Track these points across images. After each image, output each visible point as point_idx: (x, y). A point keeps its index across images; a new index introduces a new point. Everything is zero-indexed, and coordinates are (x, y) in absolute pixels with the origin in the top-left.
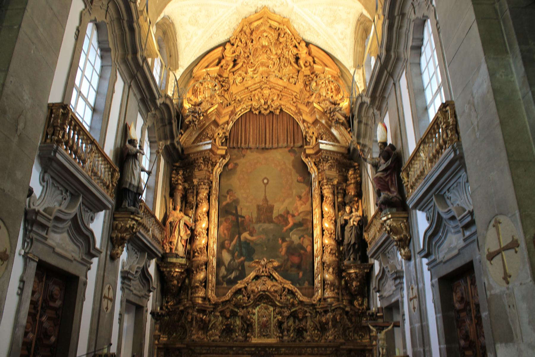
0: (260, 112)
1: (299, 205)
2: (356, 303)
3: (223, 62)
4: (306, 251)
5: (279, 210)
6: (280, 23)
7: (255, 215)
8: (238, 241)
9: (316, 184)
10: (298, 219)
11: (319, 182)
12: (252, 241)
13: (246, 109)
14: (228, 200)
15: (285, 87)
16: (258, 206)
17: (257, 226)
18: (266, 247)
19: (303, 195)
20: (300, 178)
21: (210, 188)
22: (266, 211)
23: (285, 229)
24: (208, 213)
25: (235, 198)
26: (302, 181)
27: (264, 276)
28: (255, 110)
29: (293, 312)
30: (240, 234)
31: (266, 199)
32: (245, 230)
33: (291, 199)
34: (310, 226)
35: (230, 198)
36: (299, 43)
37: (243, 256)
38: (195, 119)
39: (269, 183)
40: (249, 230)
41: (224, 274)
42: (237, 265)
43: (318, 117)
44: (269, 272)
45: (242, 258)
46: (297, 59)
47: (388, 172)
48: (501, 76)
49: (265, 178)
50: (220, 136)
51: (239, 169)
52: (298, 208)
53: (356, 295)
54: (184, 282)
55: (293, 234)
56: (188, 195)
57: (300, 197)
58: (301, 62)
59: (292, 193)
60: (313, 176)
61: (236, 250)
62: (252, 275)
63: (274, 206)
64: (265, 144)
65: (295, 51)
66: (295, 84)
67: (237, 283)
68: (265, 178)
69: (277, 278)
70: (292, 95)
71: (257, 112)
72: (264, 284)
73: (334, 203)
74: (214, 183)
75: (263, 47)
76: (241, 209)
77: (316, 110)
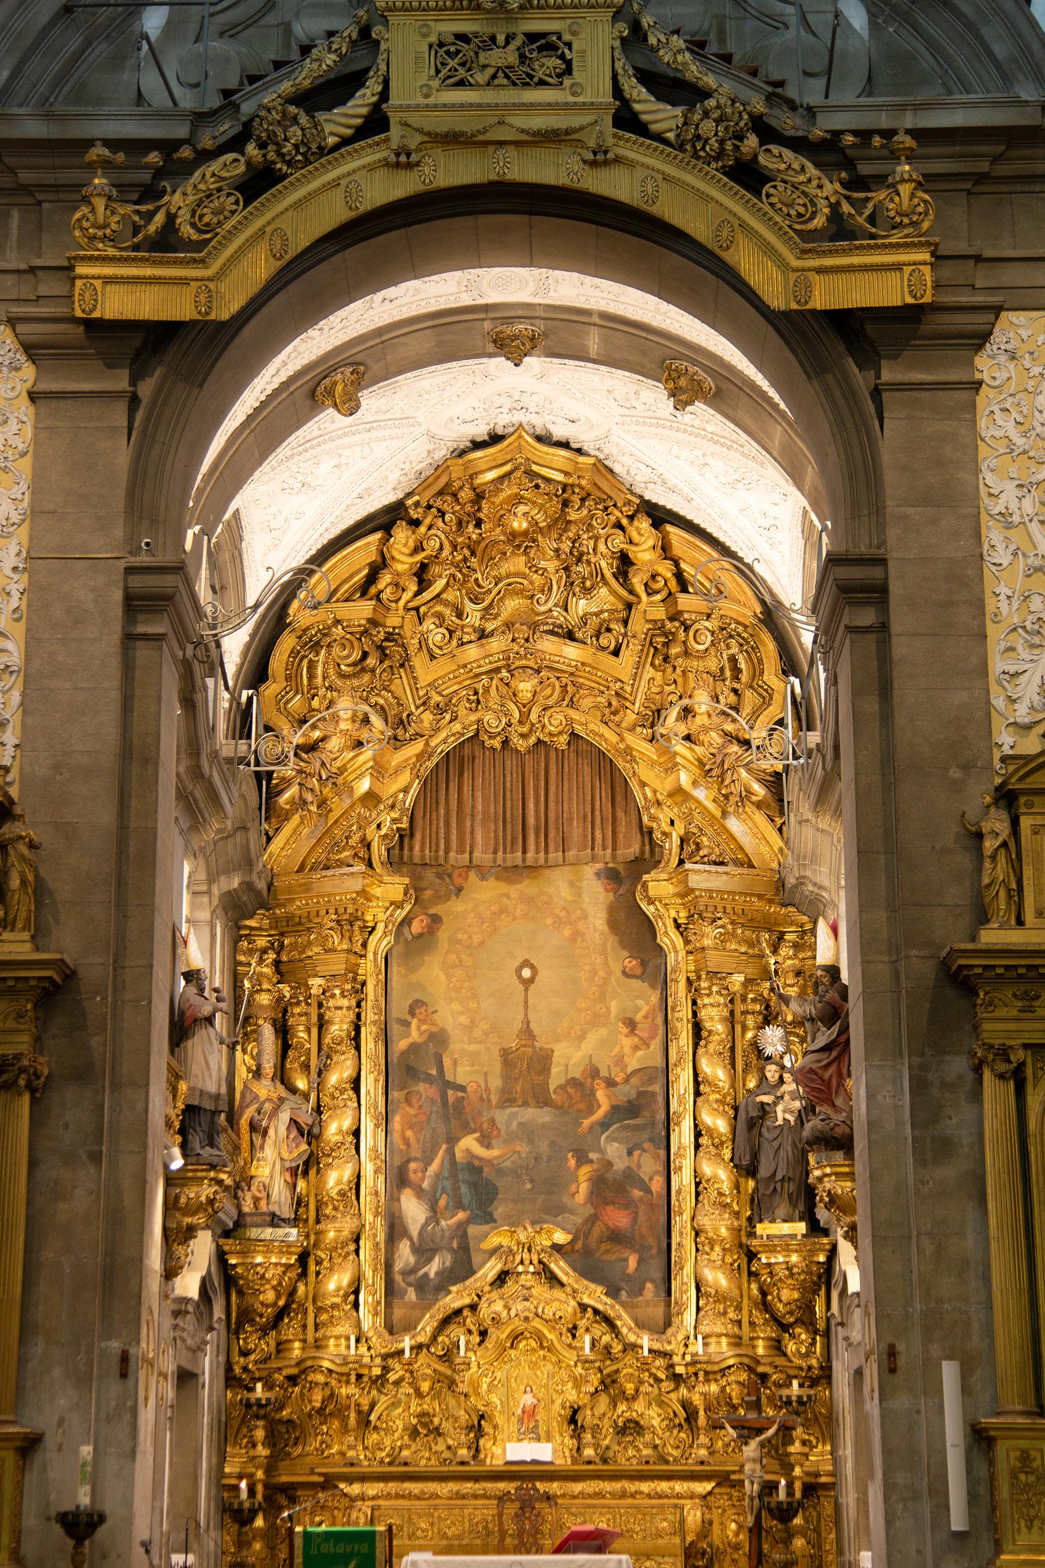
0: (505, 743)
1: (627, 1050)
2: (791, 1347)
3: (385, 579)
4: (648, 1190)
6: (566, 474)
7: (496, 1082)
8: (447, 1165)
9: (679, 991)
10: (625, 1093)
11: (689, 981)
12: (489, 1162)
13: (463, 735)
14: (415, 1034)
15: (583, 664)
16: (505, 1053)
17: (501, 1117)
18: (532, 1181)
19: (639, 1017)
20: (631, 964)
21: (359, 1005)
22: (529, 1066)
23: (586, 1123)
24: (356, 1084)
25: (434, 1029)
27: (527, 1272)
28: (490, 738)
29: (609, 1375)
30: (452, 1141)
31: (527, 1032)
32: (467, 1129)
33: (603, 1032)
34: (661, 1116)
35: (419, 1028)
36: (631, 518)
37: (464, 1210)
38: (309, 797)
41: (407, 1263)
42: (447, 1234)
43: (685, 779)
44: (540, 1262)
45: (461, 1215)
46: (625, 561)
47: (834, 1054)
48: (885, 1097)
49: (526, 963)
50: (383, 832)
51: (443, 935)
53: (792, 1325)
54: (293, 1293)
55: (611, 1139)
56: (291, 1021)
57: (631, 1025)
58: (637, 582)
59: (609, 1010)
60: (671, 959)
61: (443, 1192)
62: (491, 1269)
63: (553, 1051)
64: (524, 852)
65: (618, 542)
66: (616, 653)
67: (450, 1292)
68: (526, 963)
70: (608, 688)
71: (497, 743)
72: (526, 1299)
73: (733, 1049)
74: (370, 987)
75: (513, 535)
76: (455, 1063)
77: (679, 760)
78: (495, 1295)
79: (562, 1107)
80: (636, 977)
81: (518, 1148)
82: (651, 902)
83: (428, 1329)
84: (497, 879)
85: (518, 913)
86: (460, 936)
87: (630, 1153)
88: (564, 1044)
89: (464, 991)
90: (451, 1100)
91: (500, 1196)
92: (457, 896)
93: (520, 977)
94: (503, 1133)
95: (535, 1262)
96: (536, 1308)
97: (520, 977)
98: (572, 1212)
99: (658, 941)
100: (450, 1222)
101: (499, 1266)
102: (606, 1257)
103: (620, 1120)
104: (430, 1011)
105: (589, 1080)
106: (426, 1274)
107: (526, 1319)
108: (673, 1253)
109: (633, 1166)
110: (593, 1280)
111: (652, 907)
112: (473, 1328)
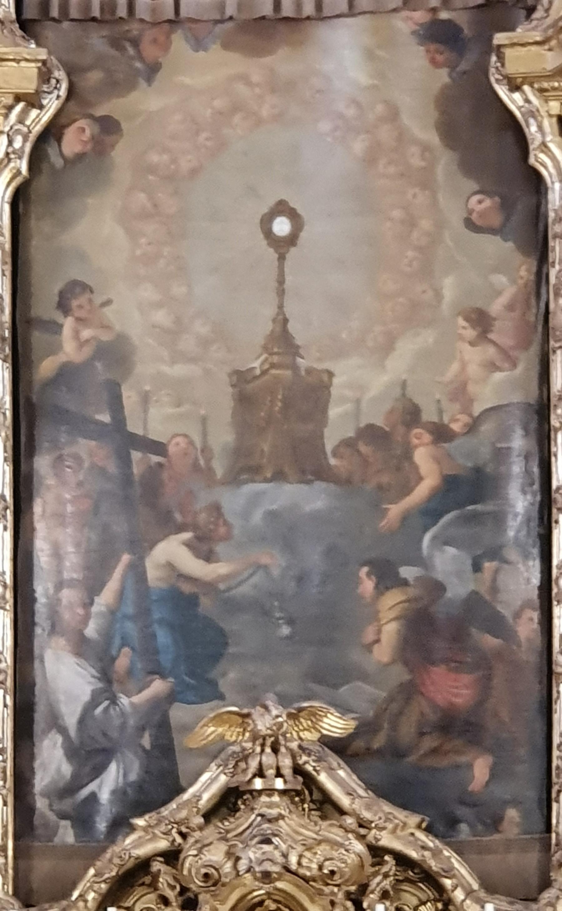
1: (473, 370)
5: (358, 402)
8: (130, 595)
18: (290, 622)
25: (106, 337)
26: (496, 220)
27: (270, 791)
35: (76, 334)
37: (163, 676)
39: (303, 235)
40: (195, 527)
42: (131, 722)
44: (298, 770)
52: (471, 388)
59: (438, 295)
63: (331, 374)
67: (133, 828)
69: (345, 801)
78: (211, 833)
79: (348, 482)
80: (492, 231)
81: (265, 560)
82: (515, 87)
83: (91, 896)
84: (226, 46)
85: (265, 112)
86: (154, 158)
87: (477, 567)
88: (354, 361)
89: (162, 263)
90: (136, 470)
91: (231, 650)
92: (149, 80)
93: (268, 234)
94: (236, 532)
95: (287, 771)
96: (285, 856)
97: (268, 234)
98: (364, 677)
99: (532, 161)
100: (136, 699)
101: (223, 779)
102: (431, 762)
103: (460, 505)
104: (98, 299)
105: (401, 429)
106: (93, 797)
107: (266, 876)
108: (18, 656)
109: (483, 590)
110: (404, 806)
111: (517, 96)
112: (171, 895)
